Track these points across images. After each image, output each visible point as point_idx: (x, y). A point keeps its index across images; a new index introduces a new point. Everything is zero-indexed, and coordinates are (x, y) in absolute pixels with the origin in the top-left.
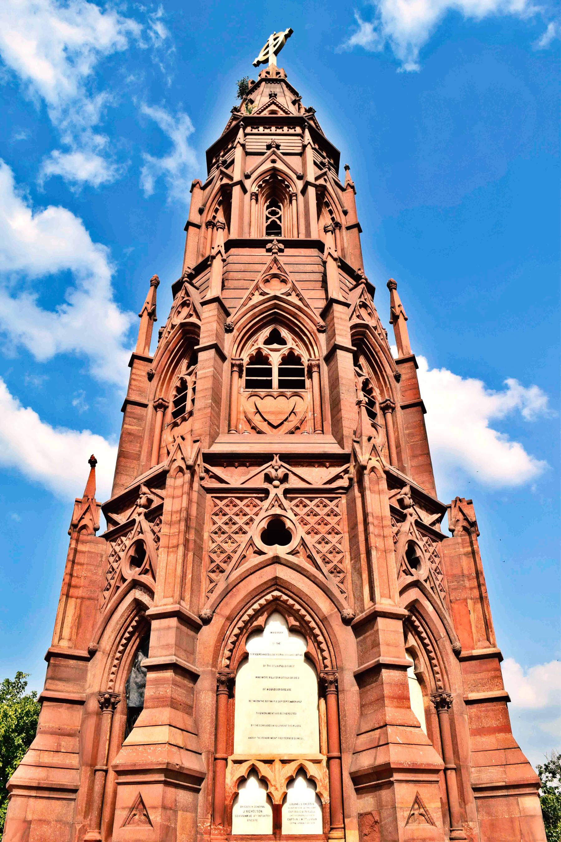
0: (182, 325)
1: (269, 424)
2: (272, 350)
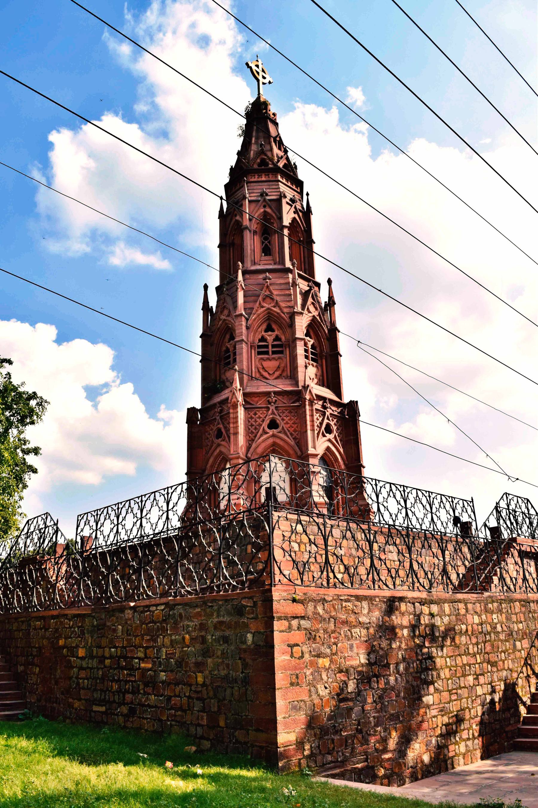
0: (225, 320)
1: (269, 373)
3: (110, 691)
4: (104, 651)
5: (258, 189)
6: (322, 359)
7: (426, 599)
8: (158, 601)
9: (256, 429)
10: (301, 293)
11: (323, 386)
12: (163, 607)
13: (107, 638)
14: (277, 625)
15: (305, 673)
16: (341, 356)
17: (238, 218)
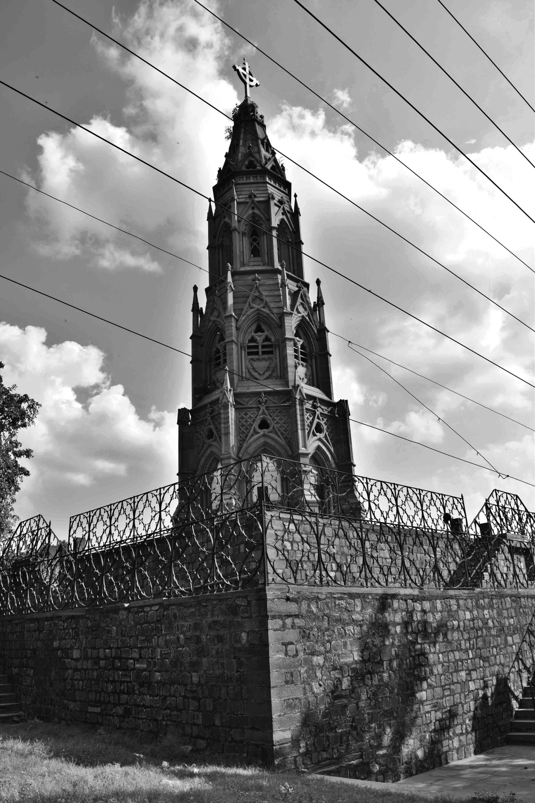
0: (215, 321)
2: (258, 336)
3: (104, 692)
4: (98, 652)
5: (247, 190)
6: (311, 359)
7: (418, 596)
8: (152, 601)
9: (247, 429)
10: (290, 293)
11: (313, 386)
12: (157, 608)
13: (102, 639)
14: (271, 624)
15: (300, 671)
16: (330, 356)
17: (227, 220)
